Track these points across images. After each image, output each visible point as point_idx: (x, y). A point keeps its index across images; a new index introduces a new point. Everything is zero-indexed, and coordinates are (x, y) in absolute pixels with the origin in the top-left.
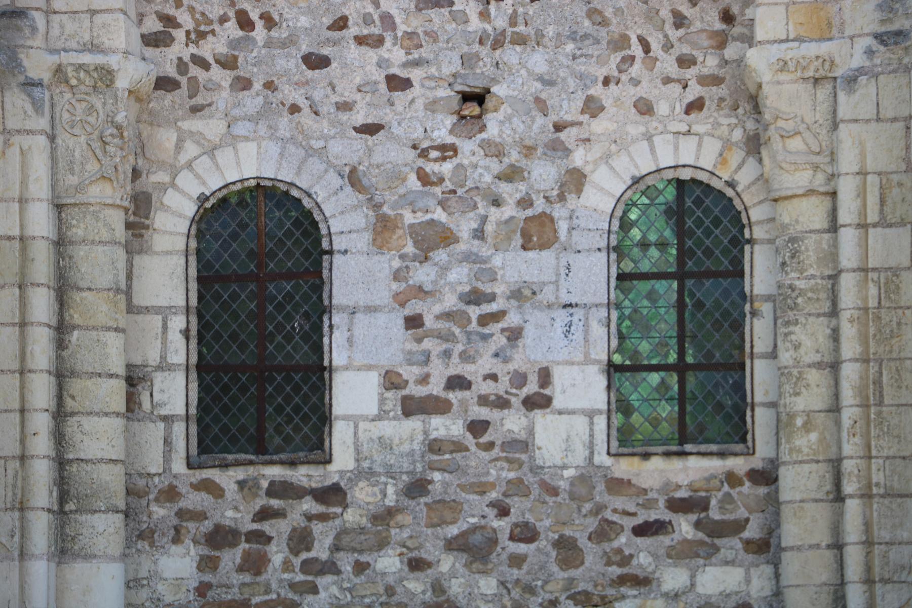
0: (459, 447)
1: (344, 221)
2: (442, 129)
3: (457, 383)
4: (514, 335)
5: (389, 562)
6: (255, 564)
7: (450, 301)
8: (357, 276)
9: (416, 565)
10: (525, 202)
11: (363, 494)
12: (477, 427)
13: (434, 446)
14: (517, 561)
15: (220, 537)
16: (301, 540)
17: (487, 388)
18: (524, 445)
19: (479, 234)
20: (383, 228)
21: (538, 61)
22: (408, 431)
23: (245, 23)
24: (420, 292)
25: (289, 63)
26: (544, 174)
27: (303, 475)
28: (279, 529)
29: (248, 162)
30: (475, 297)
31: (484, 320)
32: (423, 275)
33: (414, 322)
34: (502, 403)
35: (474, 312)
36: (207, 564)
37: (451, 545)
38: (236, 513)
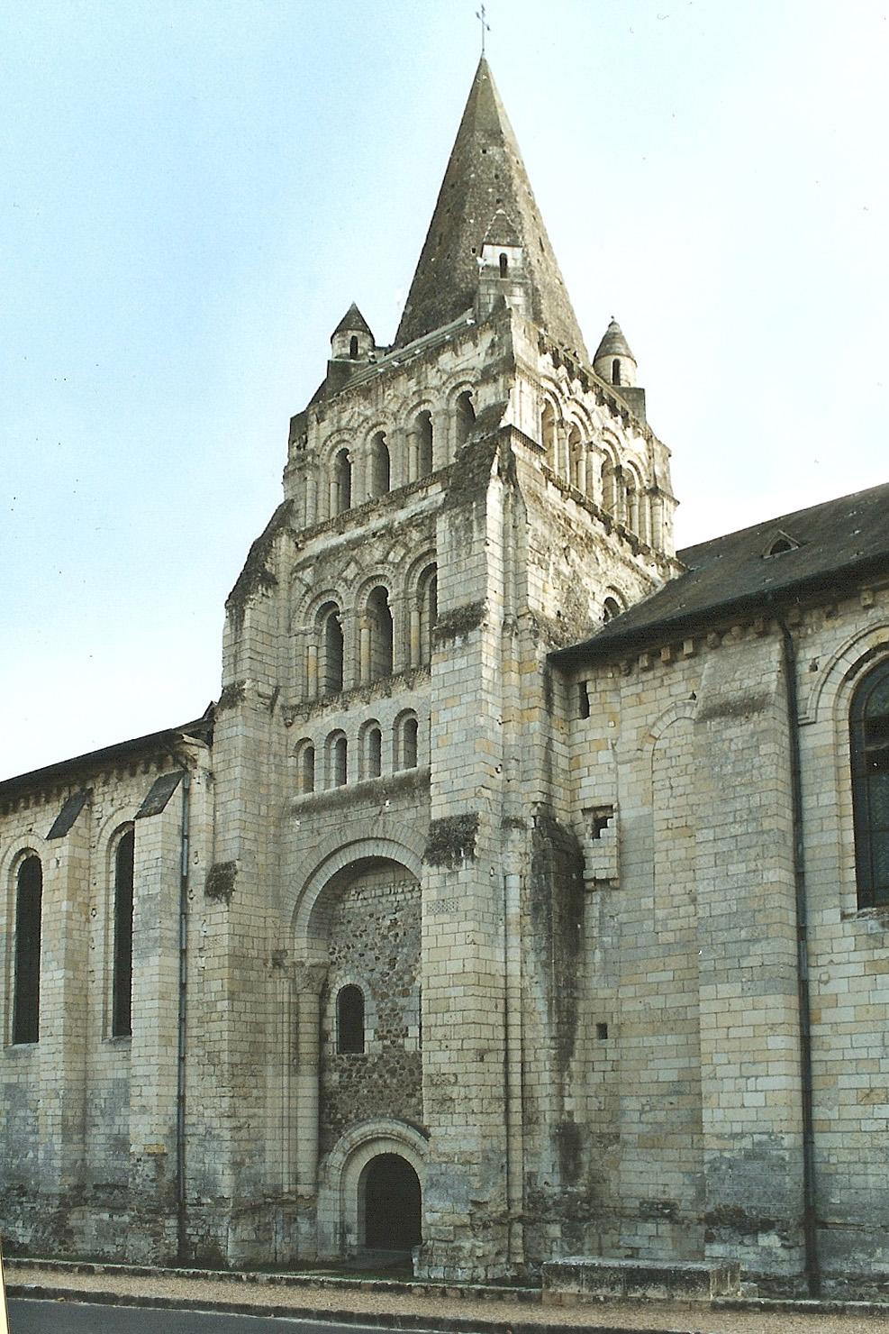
0: (388, 1047)
1: (367, 993)
2: (386, 968)
3: (389, 1031)
4: (401, 1019)
5: (375, 1076)
6: (350, 1077)
7: (387, 1012)
8: (370, 1006)
9: (381, 1076)
10: (403, 986)
11: (370, 1060)
12: (393, 1042)
13: (384, 1047)
14: (401, 1075)
15: (343, 1071)
16: (358, 1071)
17: (394, 1032)
18: (403, 1046)
19: (393, 994)
20: (374, 994)
21: (405, 950)
22: (378, 1045)
23: (349, 948)
24: (382, 1009)
25: (357, 956)
26: (406, 978)
27: (360, 1055)
28: (354, 1068)
29: (348, 981)
30: (393, 1010)
31: (395, 1016)
32: (382, 1005)
33: (380, 1017)
34: (398, 1036)
35: (392, 1014)
36: (341, 1077)
37: (387, 1071)
38: (346, 1065)
